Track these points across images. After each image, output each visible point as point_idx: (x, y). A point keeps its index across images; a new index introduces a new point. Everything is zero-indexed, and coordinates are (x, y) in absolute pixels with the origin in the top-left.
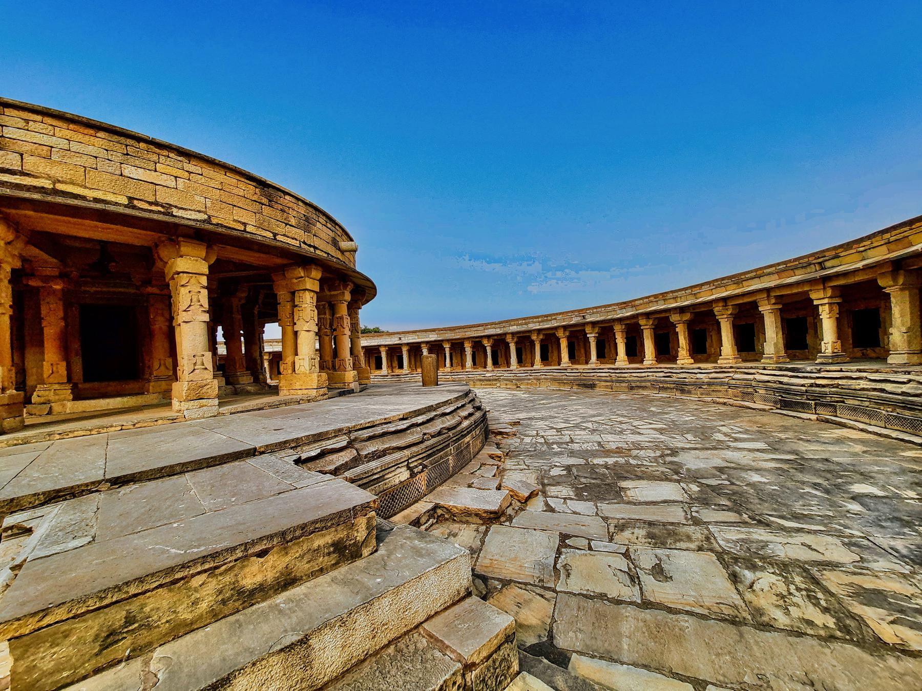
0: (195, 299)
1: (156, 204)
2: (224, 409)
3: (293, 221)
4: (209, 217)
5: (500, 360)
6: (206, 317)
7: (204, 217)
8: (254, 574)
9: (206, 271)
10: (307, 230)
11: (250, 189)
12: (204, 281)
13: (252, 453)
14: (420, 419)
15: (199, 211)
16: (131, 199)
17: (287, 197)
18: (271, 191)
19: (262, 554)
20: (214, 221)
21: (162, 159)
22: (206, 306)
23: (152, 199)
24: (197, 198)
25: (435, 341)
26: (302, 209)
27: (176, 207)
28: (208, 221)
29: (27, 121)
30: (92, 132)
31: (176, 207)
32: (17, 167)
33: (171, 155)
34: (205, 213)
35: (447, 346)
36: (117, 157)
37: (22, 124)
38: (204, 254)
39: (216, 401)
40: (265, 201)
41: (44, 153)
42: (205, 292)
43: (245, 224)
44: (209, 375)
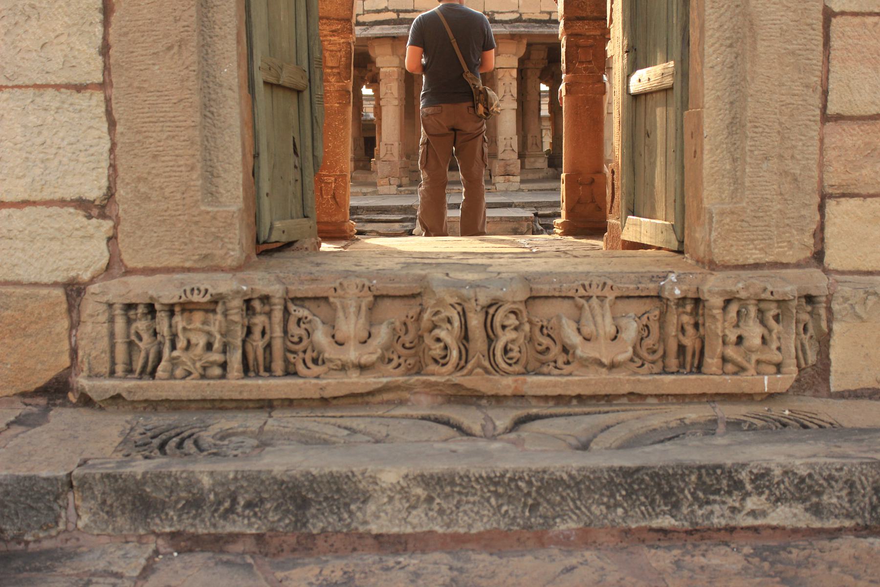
0: (508, 90)
2: (523, 186)
6: (515, 105)
7: (515, 16)
9: (516, 65)
12: (514, 73)
15: (512, 12)
20: (524, 17)
22: (515, 95)
27: (497, 12)
28: (519, 20)
31: (497, 12)
32: (411, 8)
34: (517, 12)
38: (514, 51)
42: (515, 84)
44: (515, 156)
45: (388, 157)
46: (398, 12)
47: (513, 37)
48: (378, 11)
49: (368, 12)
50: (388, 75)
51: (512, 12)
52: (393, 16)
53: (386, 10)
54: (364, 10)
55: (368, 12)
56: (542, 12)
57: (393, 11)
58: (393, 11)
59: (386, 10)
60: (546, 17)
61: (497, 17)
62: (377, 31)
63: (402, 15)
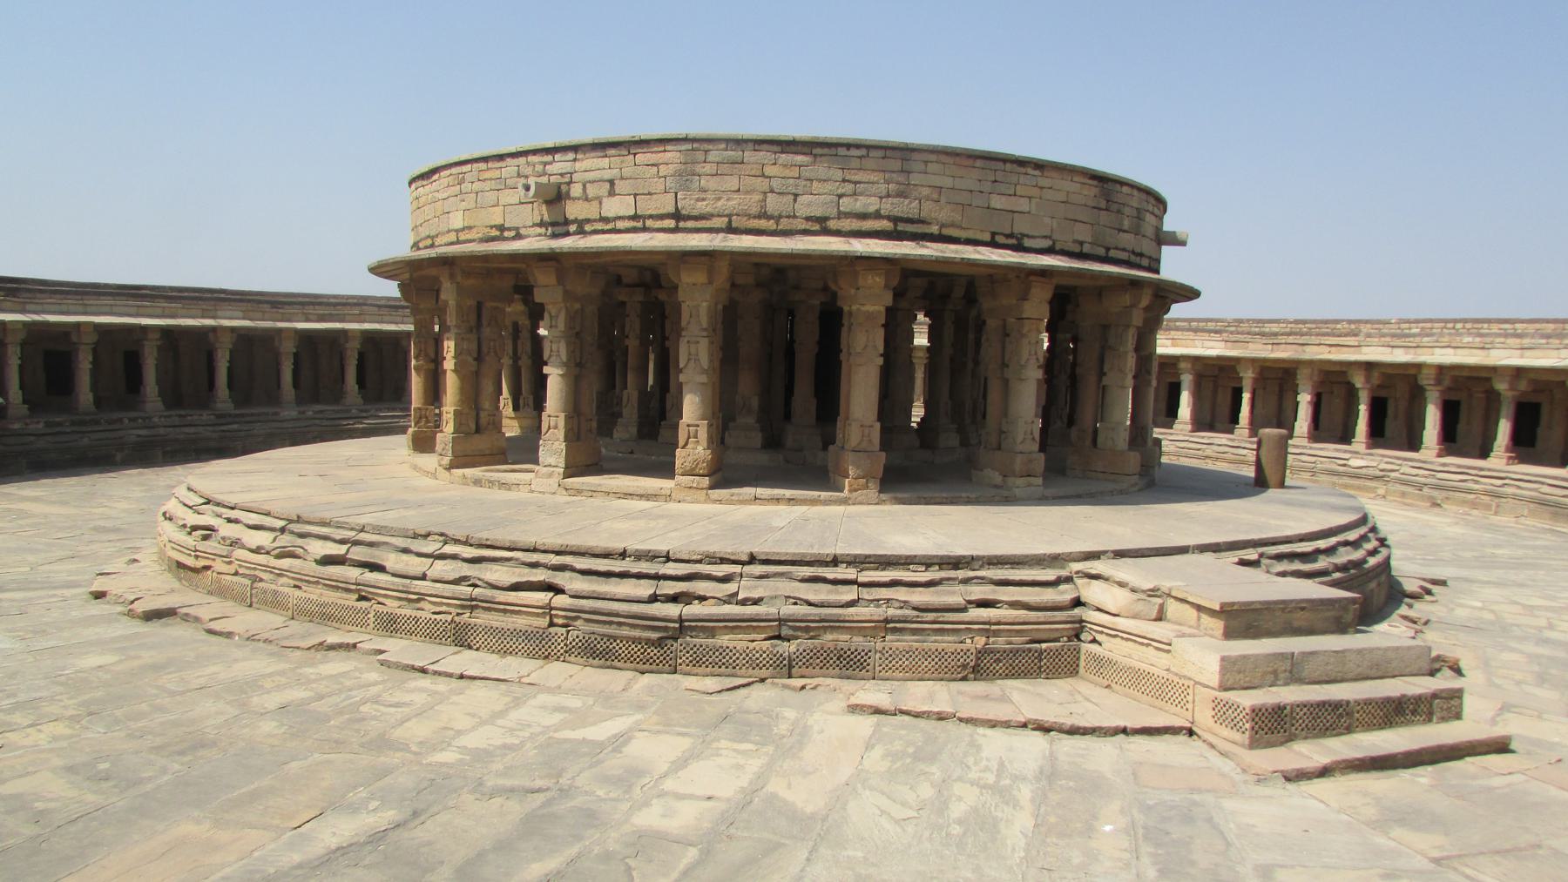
1: (1010, 236)
3: (1126, 224)
4: (1054, 242)
5: (1391, 426)
7: (1046, 243)
8: (1300, 619)
10: (1136, 231)
11: (1090, 191)
13: (1183, 550)
14: (1322, 544)
15: (1045, 237)
16: (993, 234)
17: (1125, 189)
18: (1110, 186)
19: (1303, 609)
20: (1058, 247)
21: (1022, 179)
23: (1008, 231)
24: (1047, 220)
25: (1219, 358)
26: (1136, 200)
27: (1028, 236)
29: (926, 162)
30: (970, 162)
31: (1028, 236)
33: (1030, 171)
35: (1248, 377)
36: (987, 187)
37: (921, 167)
39: (1039, 481)
40: (1103, 204)
41: (935, 196)
43: (1081, 243)
44: (1036, 447)
45: (864, 445)
46: (896, 220)
47: (1044, 272)
48: (863, 216)
49: (848, 215)
50: (870, 316)
51: (1045, 237)
52: (885, 225)
53: (877, 215)
54: (840, 213)
55: (848, 215)
56: (1075, 241)
57: (889, 218)
58: (889, 218)
59: (877, 215)
60: (1077, 249)
61: (1027, 243)
62: (860, 246)
63: (901, 227)
